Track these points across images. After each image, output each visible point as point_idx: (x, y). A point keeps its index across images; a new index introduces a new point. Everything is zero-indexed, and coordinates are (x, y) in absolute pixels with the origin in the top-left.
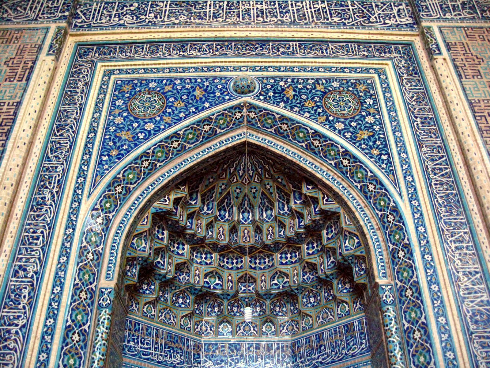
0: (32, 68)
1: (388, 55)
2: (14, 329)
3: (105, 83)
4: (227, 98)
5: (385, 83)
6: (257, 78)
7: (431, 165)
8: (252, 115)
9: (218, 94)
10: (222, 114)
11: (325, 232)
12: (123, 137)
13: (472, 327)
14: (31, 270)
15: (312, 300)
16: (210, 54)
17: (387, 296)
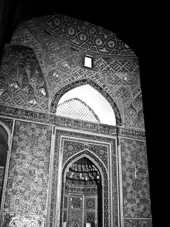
0: (51, 137)
1: (111, 141)
2: (54, 190)
3: (62, 141)
4: (84, 148)
5: (109, 148)
6: (89, 144)
7: (113, 167)
8: (87, 152)
9: (82, 147)
10: (83, 152)
11: (94, 173)
12: (67, 155)
13: (114, 194)
14: (55, 180)
15: (88, 182)
16: (81, 137)
17: (103, 188)
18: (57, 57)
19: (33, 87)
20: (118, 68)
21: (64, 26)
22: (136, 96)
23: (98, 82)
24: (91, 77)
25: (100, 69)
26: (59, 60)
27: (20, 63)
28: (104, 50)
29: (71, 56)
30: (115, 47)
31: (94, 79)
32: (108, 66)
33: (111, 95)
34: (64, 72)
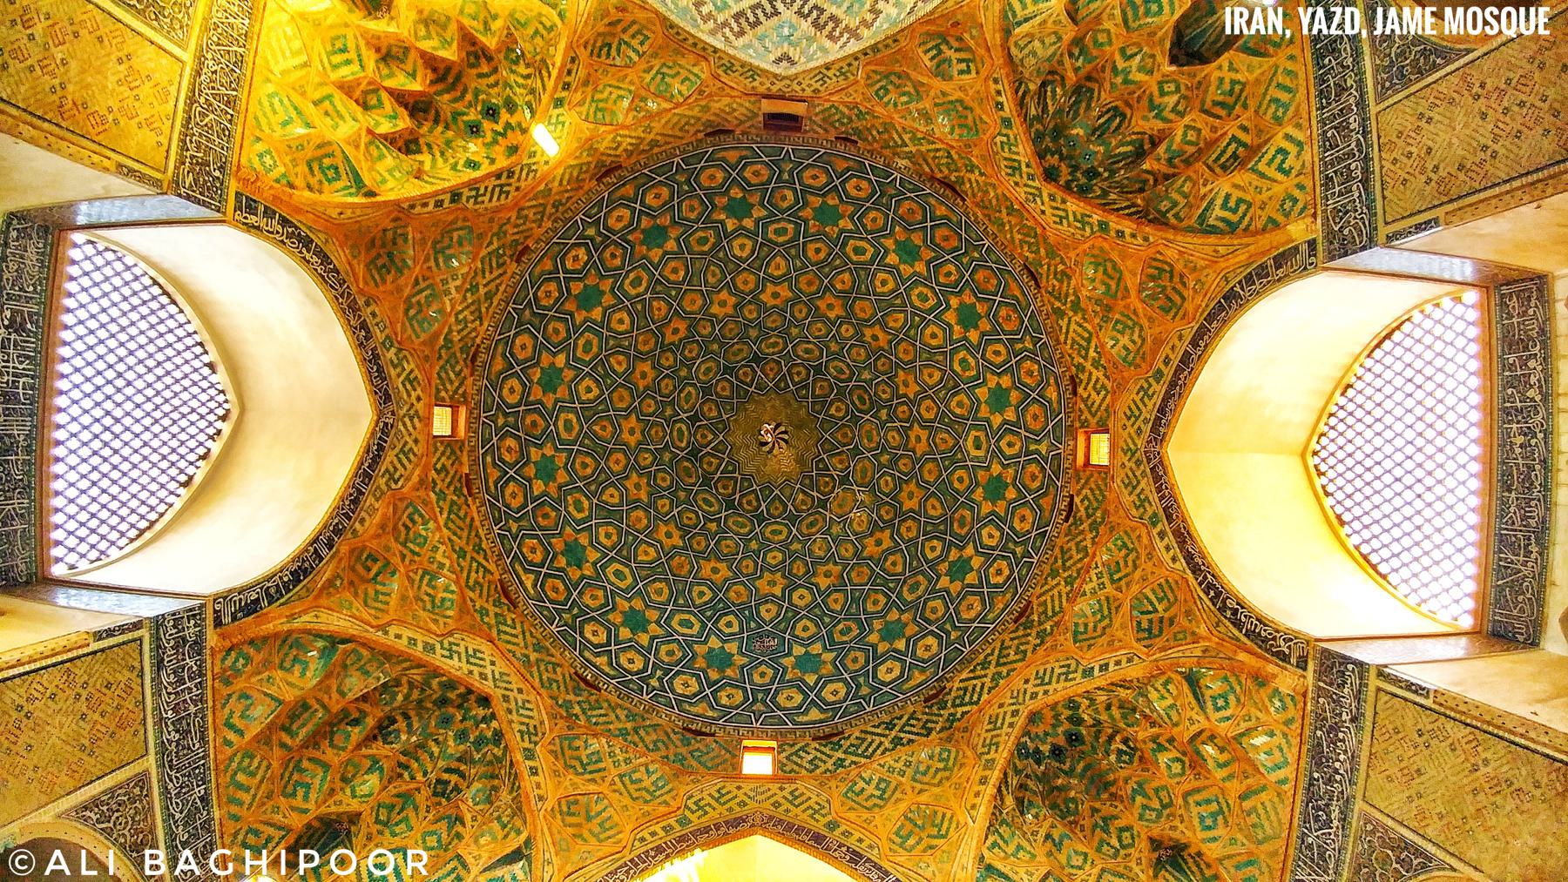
18: (618, 751)
19: (469, 860)
20: (874, 746)
21: (659, 673)
22: (982, 809)
23: (804, 816)
24: (767, 805)
25: (804, 772)
26: (627, 761)
27: (446, 776)
28: (815, 714)
29: (683, 750)
30: (847, 694)
31: (781, 809)
32: (840, 755)
33: (873, 855)
34: (646, 802)
